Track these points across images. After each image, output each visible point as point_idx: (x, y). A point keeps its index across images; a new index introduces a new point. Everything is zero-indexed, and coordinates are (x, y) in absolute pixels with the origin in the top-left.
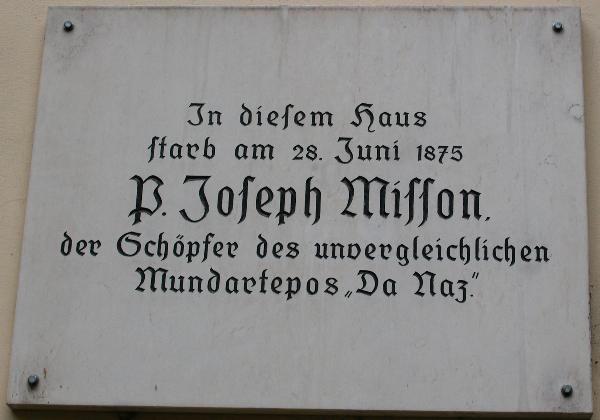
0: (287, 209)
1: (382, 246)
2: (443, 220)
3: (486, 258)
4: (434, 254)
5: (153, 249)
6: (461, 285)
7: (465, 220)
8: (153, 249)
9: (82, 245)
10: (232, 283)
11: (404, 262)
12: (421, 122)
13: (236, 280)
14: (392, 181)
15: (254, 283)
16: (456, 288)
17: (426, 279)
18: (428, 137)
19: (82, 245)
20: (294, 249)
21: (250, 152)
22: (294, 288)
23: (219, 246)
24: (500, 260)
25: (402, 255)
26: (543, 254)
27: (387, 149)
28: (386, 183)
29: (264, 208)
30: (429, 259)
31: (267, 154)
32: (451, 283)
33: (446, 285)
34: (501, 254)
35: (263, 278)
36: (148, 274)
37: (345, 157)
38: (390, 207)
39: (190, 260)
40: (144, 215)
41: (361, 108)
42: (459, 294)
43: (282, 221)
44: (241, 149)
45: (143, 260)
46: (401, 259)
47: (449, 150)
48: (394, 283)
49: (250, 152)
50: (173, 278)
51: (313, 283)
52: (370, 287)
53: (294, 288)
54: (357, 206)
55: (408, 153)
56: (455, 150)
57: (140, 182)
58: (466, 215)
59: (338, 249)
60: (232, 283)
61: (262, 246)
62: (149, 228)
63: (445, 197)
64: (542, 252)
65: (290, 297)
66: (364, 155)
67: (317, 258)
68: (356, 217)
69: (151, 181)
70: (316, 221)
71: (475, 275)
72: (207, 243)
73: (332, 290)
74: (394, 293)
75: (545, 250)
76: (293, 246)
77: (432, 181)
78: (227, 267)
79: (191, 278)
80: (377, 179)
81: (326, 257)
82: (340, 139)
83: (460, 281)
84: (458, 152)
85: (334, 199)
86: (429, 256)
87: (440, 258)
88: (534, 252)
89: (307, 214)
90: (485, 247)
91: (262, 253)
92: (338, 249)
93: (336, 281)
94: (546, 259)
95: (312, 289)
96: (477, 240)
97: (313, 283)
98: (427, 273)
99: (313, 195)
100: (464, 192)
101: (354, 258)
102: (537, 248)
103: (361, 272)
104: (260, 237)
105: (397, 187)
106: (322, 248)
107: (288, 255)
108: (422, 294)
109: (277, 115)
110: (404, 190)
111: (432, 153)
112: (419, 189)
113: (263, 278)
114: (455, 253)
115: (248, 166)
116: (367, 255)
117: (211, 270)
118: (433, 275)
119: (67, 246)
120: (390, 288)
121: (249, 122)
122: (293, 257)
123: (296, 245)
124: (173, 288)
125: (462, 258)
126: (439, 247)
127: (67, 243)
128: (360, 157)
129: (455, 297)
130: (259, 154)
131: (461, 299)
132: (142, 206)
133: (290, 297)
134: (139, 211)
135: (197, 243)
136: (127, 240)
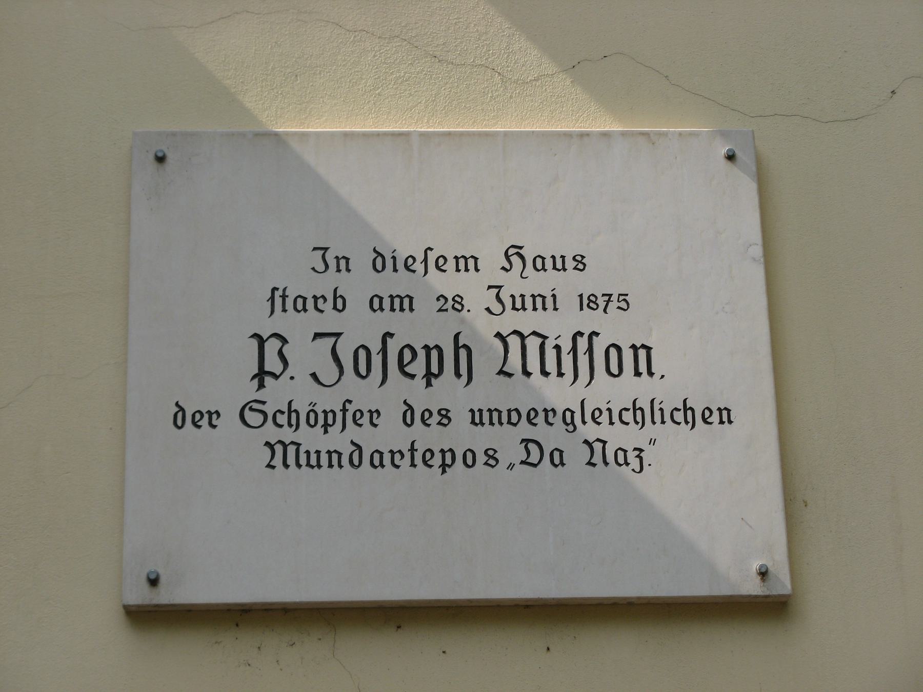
0: (435, 369)
1: (545, 410)
3: (663, 422)
4: (605, 418)
5: (282, 419)
6: (637, 453)
8: (282, 419)
9: (198, 416)
10: (377, 457)
11: (571, 428)
15: (403, 456)
16: (631, 455)
18: (587, 283)
19: (198, 416)
20: (445, 416)
22: (448, 461)
23: (358, 415)
25: (569, 420)
27: (544, 298)
32: (625, 451)
33: (621, 454)
34: (679, 416)
35: (412, 450)
36: (279, 449)
38: (551, 366)
39: (326, 432)
40: (268, 380)
43: (429, 384)
45: (271, 433)
46: (567, 424)
47: (614, 298)
48: (561, 452)
50: (308, 452)
53: (448, 461)
56: (621, 298)
58: (638, 374)
59: (495, 414)
60: (377, 457)
62: (276, 395)
63: (613, 352)
64: (725, 413)
65: (444, 471)
66: (518, 305)
68: (513, 377)
71: (652, 442)
72: (344, 410)
74: (563, 464)
75: (729, 411)
76: (444, 412)
79: (329, 452)
80: (535, 333)
83: (635, 449)
84: (624, 300)
87: (611, 423)
88: (716, 414)
89: (458, 375)
90: (661, 409)
93: (495, 451)
94: (730, 422)
95: (470, 462)
99: (463, 353)
100: (633, 347)
101: (515, 425)
103: (523, 441)
105: (558, 342)
107: (439, 423)
108: (594, 465)
110: (566, 346)
111: (594, 303)
112: (582, 343)
113: (412, 450)
114: (628, 416)
116: (529, 421)
117: (352, 442)
118: (604, 443)
119: (180, 417)
120: (558, 459)
122: (445, 425)
123: (448, 411)
125: (637, 423)
126: (609, 410)
127: (180, 415)
128: (514, 308)
131: (638, 470)
132: (267, 369)
133: (444, 471)
134: (261, 375)
135: (332, 411)
136: (251, 409)
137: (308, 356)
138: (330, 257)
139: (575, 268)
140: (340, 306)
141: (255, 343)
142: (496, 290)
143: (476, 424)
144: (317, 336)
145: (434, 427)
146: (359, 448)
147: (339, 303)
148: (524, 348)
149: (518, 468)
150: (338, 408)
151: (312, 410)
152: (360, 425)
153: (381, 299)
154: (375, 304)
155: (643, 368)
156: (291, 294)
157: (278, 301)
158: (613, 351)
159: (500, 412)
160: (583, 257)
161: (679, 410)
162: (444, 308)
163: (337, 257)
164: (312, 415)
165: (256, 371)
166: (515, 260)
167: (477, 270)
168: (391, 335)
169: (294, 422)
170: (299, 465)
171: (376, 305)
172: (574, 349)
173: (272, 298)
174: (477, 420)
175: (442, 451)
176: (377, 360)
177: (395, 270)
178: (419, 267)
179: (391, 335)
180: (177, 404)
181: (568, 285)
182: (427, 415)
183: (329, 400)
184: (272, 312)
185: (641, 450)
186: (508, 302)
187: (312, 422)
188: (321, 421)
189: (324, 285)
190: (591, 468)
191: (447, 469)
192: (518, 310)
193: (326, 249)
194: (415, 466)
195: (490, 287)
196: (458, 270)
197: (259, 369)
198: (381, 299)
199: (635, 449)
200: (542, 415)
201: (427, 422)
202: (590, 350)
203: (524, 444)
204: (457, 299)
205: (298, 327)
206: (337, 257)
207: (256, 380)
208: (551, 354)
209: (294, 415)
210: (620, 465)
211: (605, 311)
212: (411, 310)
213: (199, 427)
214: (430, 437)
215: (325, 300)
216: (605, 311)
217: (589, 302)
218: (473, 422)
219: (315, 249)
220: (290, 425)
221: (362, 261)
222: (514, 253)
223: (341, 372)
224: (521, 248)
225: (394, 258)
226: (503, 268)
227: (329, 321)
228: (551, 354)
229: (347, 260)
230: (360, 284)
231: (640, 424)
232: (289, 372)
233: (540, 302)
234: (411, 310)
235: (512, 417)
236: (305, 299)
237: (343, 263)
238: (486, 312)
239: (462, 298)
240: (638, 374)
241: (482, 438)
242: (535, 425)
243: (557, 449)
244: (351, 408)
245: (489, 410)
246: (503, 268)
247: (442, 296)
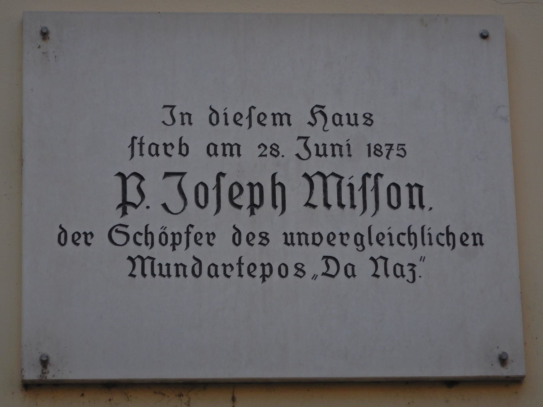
0: (257, 201)
1: (341, 234)
3: (431, 244)
4: (386, 241)
5: (141, 239)
6: (411, 267)
7: (411, 210)
8: (141, 239)
9: (76, 236)
10: (213, 269)
11: (360, 248)
12: (369, 122)
13: (216, 266)
15: (232, 268)
16: (406, 269)
17: (381, 262)
18: (376, 135)
19: (76, 236)
20: (265, 237)
22: (267, 272)
23: (199, 236)
24: (443, 245)
25: (359, 242)
26: (478, 239)
27: (341, 146)
29: (236, 201)
31: (235, 151)
32: (402, 266)
33: (398, 268)
34: (443, 240)
35: (240, 263)
36: (138, 262)
38: (346, 200)
39: (174, 249)
40: (130, 209)
41: (316, 110)
43: (252, 213)
44: (212, 148)
45: (132, 250)
46: (358, 245)
47: (395, 147)
48: (353, 266)
50: (160, 265)
51: (283, 268)
53: (267, 272)
54: (318, 198)
55: (359, 150)
56: (400, 147)
58: (412, 206)
59: (303, 237)
60: (213, 269)
62: (135, 221)
63: (393, 189)
64: (478, 237)
65: (264, 280)
66: (321, 152)
68: (317, 208)
71: (422, 259)
72: (188, 233)
74: (354, 276)
75: (481, 236)
76: (264, 235)
78: (208, 255)
79: (176, 265)
80: (333, 174)
82: (299, 138)
83: (409, 264)
84: (402, 149)
85: (297, 192)
87: (392, 244)
88: (471, 238)
89: (275, 206)
90: (429, 234)
91: (237, 242)
92: (303, 237)
93: (303, 265)
94: (482, 244)
95: (283, 273)
96: (423, 228)
97: (283, 268)
98: (381, 257)
99: (278, 189)
100: (409, 185)
101: (318, 245)
103: (324, 257)
104: (234, 227)
105: (352, 181)
107: (260, 243)
108: (378, 276)
109: (241, 116)
110: (358, 184)
111: (380, 151)
112: (370, 183)
113: (240, 263)
114: (404, 239)
116: (329, 242)
117: (194, 257)
118: (386, 259)
119: (62, 238)
120: (350, 272)
122: (265, 245)
123: (267, 234)
125: (411, 244)
126: (390, 234)
127: (63, 235)
128: (318, 154)
129: (406, 278)
130: (228, 151)
131: (411, 280)
132: (129, 200)
133: (264, 280)
134: (124, 204)
135: (179, 233)
136: (117, 231)
137: (159, 190)
138: (176, 113)
139: (365, 124)
140: (184, 152)
141: (119, 179)
142: (303, 141)
143: (289, 245)
144: (167, 175)
145: (257, 246)
146: (199, 261)
147: (184, 149)
148: (325, 185)
149: (321, 278)
150: (183, 231)
151: (164, 233)
152: (200, 244)
153: (216, 146)
154: (211, 150)
155: (416, 202)
156: (147, 142)
157: (137, 147)
158: (393, 189)
159: (306, 235)
160: (371, 115)
161: (443, 235)
162: (263, 154)
163: (182, 113)
164: (163, 236)
165: (121, 202)
166: (319, 116)
167: (289, 124)
168: (223, 175)
169: (149, 241)
170: (154, 275)
171: (212, 151)
172: (364, 187)
173: (132, 145)
174: (289, 241)
175: (263, 265)
176: (212, 194)
177: (227, 124)
178: (245, 122)
179: (223, 175)
180: (60, 227)
181: (359, 136)
182: (251, 237)
183: (176, 225)
184: (132, 156)
185: (414, 265)
186: (313, 150)
187: (163, 241)
188: (170, 241)
189: (171, 135)
190: (375, 278)
191: (266, 278)
192: (321, 156)
193: (173, 107)
194: (242, 276)
195: (299, 138)
196: (275, 124)
197: (123, 200)
198: (216, 146)
199: (409, 264)
200: (338, 237)
201: (251, 242)
202: (376, 188)
203: (324, 260)
204: (274, 147)
205: (152, 167)
206: (182, 113)
207: (120, 209)
208: (346, 191)
209: (149, 236)
210: (398, 277)
211: (387, 157)
212: (239, 155)
213: (78, 244)
214: (253, 254)
215: (173, 147)
216: (387, 157)
217: (375, 150)
218: (286, 243)
219: (165, 106)
220: (147, 244)
221: (201, 116)
222: (318, 111)
223: (186, 204)
224: (323, 107)
225: (225, 114)
226: (310, 123)
227: (176, 163)
228: (346, 191)
229: (190, 115)
230: (199, 135)
231: (413, 246)
232: (146, 202)
233: (338, 150)
234: (239, 155)
235: (316, 239)
236: (157, 146)
237: (186, 117)
238: (296, 157)
239: (278, 147)
240: (412, 206)
241: (294, 255)
242: (333, 245)
243: (350, 264)
244: (193, 231)
245: (299, 234)
246: (310, 123)
247: (262, 144)
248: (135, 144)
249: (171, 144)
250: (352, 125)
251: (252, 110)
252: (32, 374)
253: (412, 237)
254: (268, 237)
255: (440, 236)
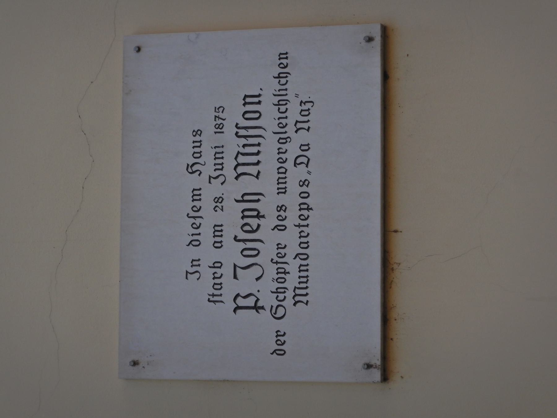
0: (255, 213)
1: (279, 153)
2: (262, 117)
3: (286, 90)
4: (284, 121)
5: (281, 296)
6: (303, 104)
7: (262, 103)
8: (281, 296)
9: (279, 342)
10: (302, 245)
11: (288, 140)
13: (301, 243)
14: (237, 149)
15: (302, 231)
16: (304, 107)
17: (299, 125)
18: (209, 128)
19: (279, 342)
20: (280, 208)
21: (218, 239)
22: (306, 206)
23: (279, 255)
24: (287, 81)
25: (284, 141)
26: (283, 56)
27: (216, 153)
28: (238, 153)
29: (255, 228)
30: (286, 124)
32: (302, 110)
33: (303, 113)
34: (283, 81)
35: (299, 226)
36: (297, 298)
37: (221, 179)
38: (254, 150)
39: (288, 273)
40: (260, 304)
42: (308, 106)
43: (263, 217)
45: (289, 302)
46: (287, 142)
47: (217, 114)
48: (302, 145)
49: (218, 239)
50: (300, 283)
51: (302, 195)
52: (305, 160)
53: (306, 206)
54: (253, 170)
56: (217, 111)
57: (238, 308)
58: (259, 103)
59: (280, 181)
60: (302, 245)
61: (279, 228)
62: (268, 300)
64: (282, 56)
65: (311, 209)
66: (220, 167)
67: (287, 193)
69: (237, 301)
70: (263, 195)
71: (297, 96)
72: (277, 263)
73: (306, 183)
74: (308, 145)
75: (281, 54)
76: (279, 209)
77: (237, 124)
78: (293, 249)
79: (300, 271)
80: (236, 158)
81: (286, 188)
83: (301, 105)
84: (218, 109)
85: (248, 185)
86: (284, 125)
87: (286, 117)
88: (282, 61)
89: (258, 200)
90: (279, 90)
91: (283, 228)
92: (280, 181)
93: (301, 181)
94: (287, 53)
95: (306, 195)
96: (275, 95)
97: (302, 195)
98: (295, 125)
99: (246, 198)
100: (244, 105)
101: (286, 170)
102: (280, 59)
103: (295, 166)
104: (273, 230)
105: (241, 145)
106: (280, 190)
107: (285, 211)
108: (309, 128)
110: (243, 141)
111: (219, 125)
112: (242, 132)
113: (299, 226)
114: (283, 109)
115: (227, 239)
116: (284, 162)
117: (294, 259)
118: (297, 122)
121: (198, 240)
122: (286, 208)
123: (278, 206)
124: (306, 282)
126: (279, 119)
127: (278, 352)
128: (222, 169)
129: (310, 107)
131: (312, 104)
132: (253, 305)
133: (311, 209)
134: (256, 308)
135: (277, 269)
136: (275, 314)
137: (247, 282)
138: (192, 270)
139: (200, 135)
140: (219, 265)
141: (239, 311)
142: (212, 179)
143: (286, 191)
144: (235, 277)
145: (286, 214)
148: (244, 164)
149: (310, 168)
150: (276, 266)
151: (277, 280)
152: (285, 254)
153: (215, 242)
154: (218, 245)
155: (256, 100)
157: (216, 298)
160: (194, 131)
161: (280, 81)
162: (221, 208)
163: (192, 266)
165: (254, 310)
169: (282, 290)
170: (307, 288)
171: (219, 245)
172: (245, 137)
173: (214, 302)
174: (284, 190)
176: (250, 245)
177: (199, 234)
178: (198, 221)
179: (236, 237)
180: (272, 354)
181: (209, 140)
182: (280, 218)
183: (271, 271)
184: (222, 302)
185: (301, 102)
187: (283, 280)
188: (283, 275)
191: (310, 207)
192: (223, 167)
193: (187, 272)
195: (210, 182)
196: (200, 200)
198: (215, 242)
200: (281, 155)
205: (230, 288)
206: (192, 266)
207: (260, 311)
208: (248, 150)
211: (224, 120)
212: (222, 226)
215: (215, 273)
216: (224, 120)
218: (285, 193)
219: (187, 278)
221: (194, 252)
222: (191, 169)
224: (188, 165)
225: (192, 235)
226: (199, 175)
227: (227, 271)
228: (248, 150)
229: (193, 260)
230: (207, 254)
231: (287, 102)
233: (218, 155)
234: (222, 226)
235: (282, 172)
236: (215, 284)
237: (194, 263)
238: (224, 185)
239: (216, 198)
240: (259, 103)
243: (300, 148)
244: (276, 259)
245: (278, 184)
246: (199, 175)
247: (214, 209)
248: (214, 299)
249: (214, 274)
250: (201, 144)
251: (189, 216)
252: (377, 375)
253: (281, 103)
254: (280, 206)
255: (281, 83)
